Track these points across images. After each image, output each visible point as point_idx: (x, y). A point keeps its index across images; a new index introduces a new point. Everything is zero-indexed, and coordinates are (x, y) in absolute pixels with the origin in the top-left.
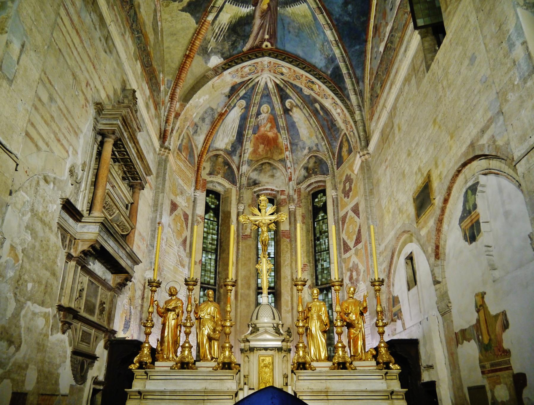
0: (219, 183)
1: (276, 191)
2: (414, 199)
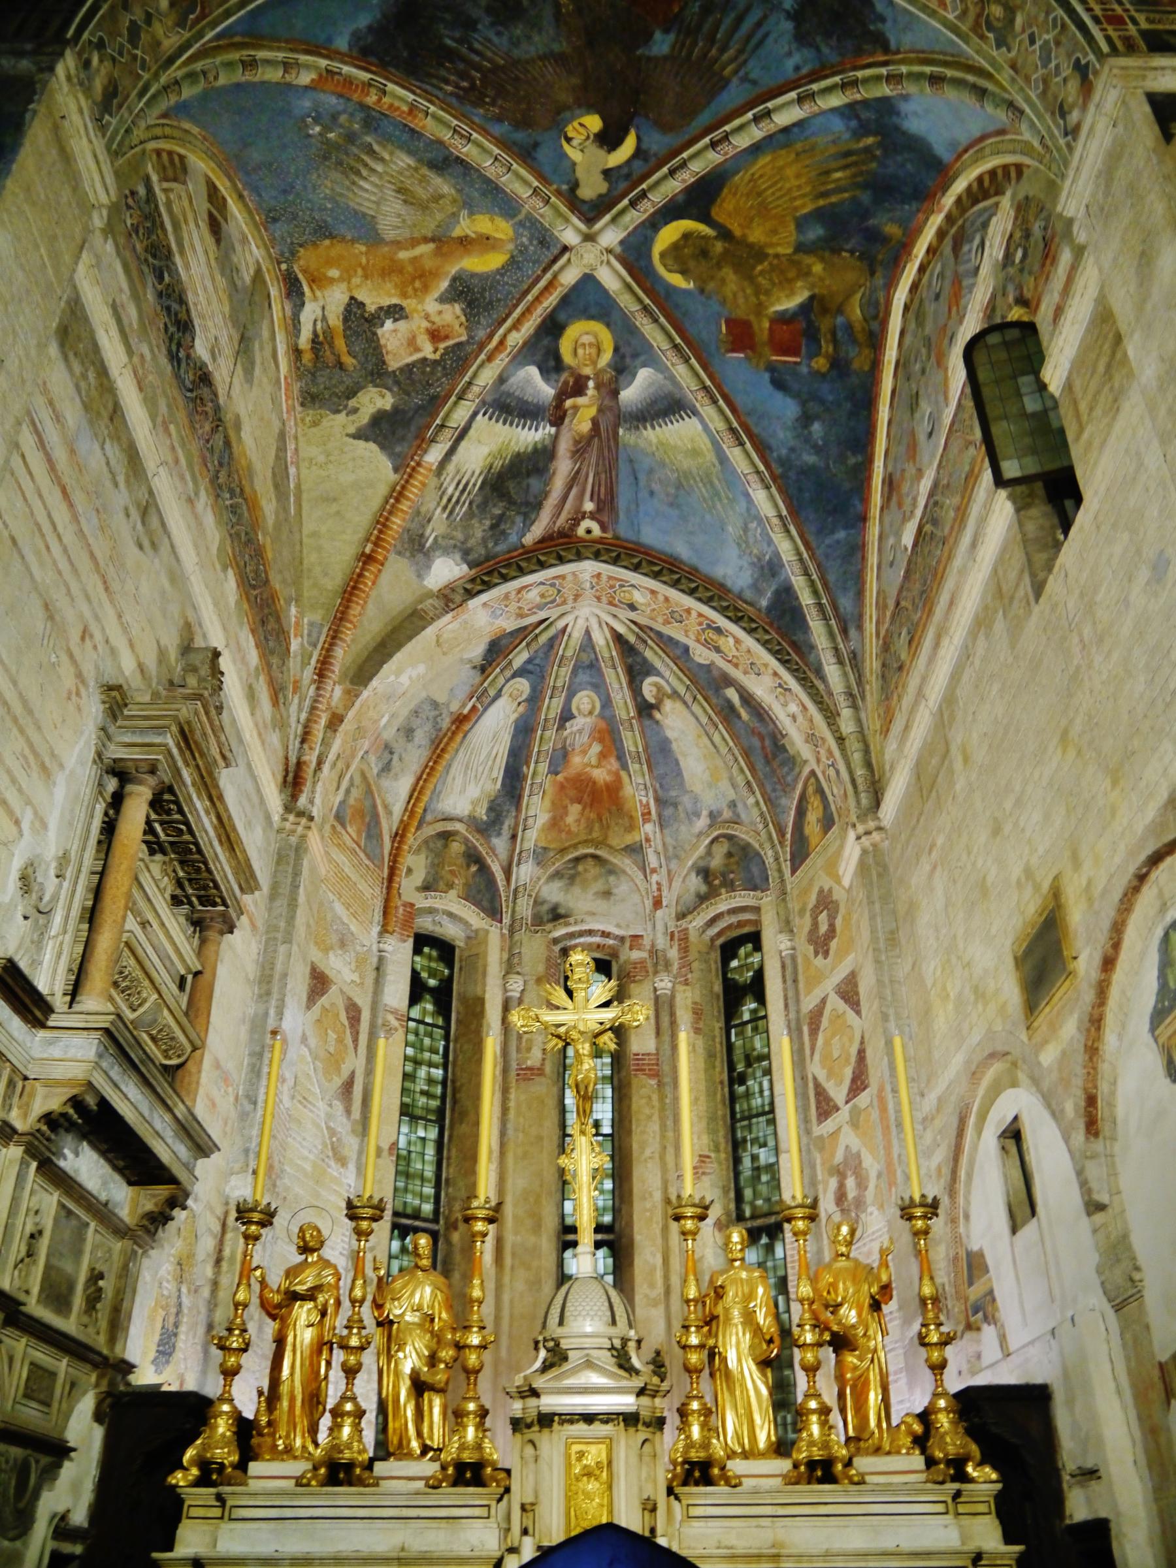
0: (450, 915)
1: (616, 937)
2: (1016, 958)
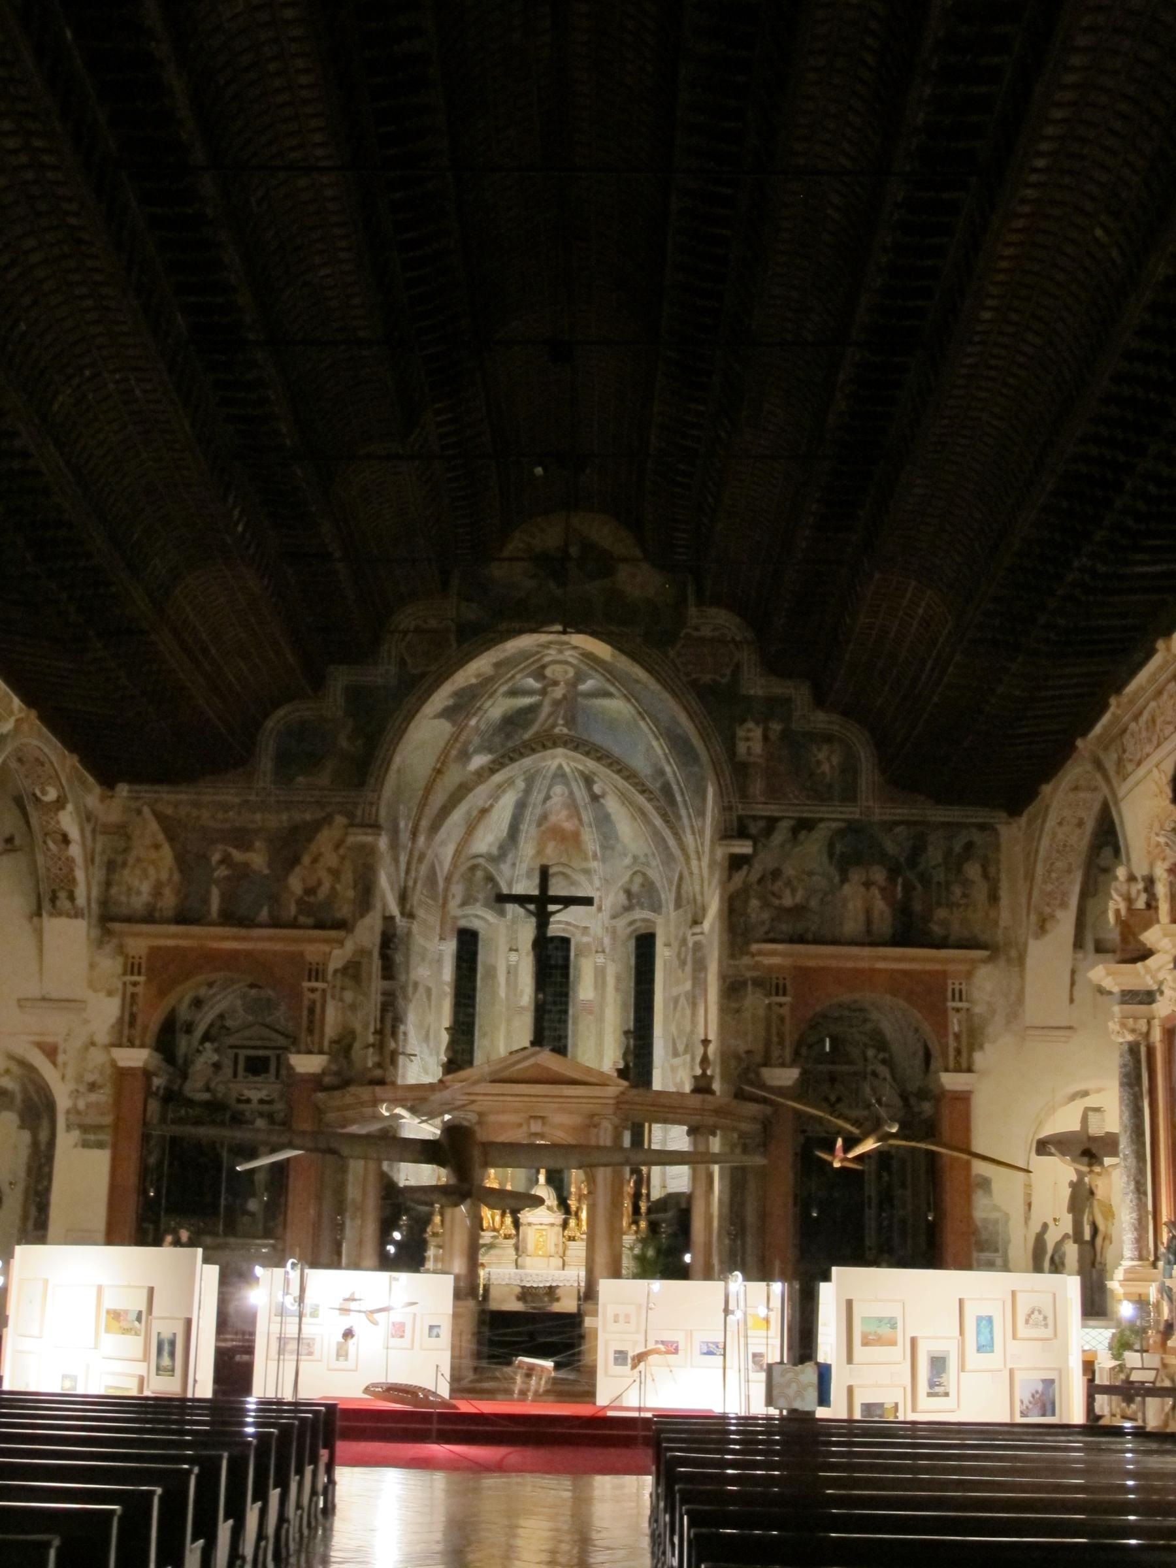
0: (477, 916)
